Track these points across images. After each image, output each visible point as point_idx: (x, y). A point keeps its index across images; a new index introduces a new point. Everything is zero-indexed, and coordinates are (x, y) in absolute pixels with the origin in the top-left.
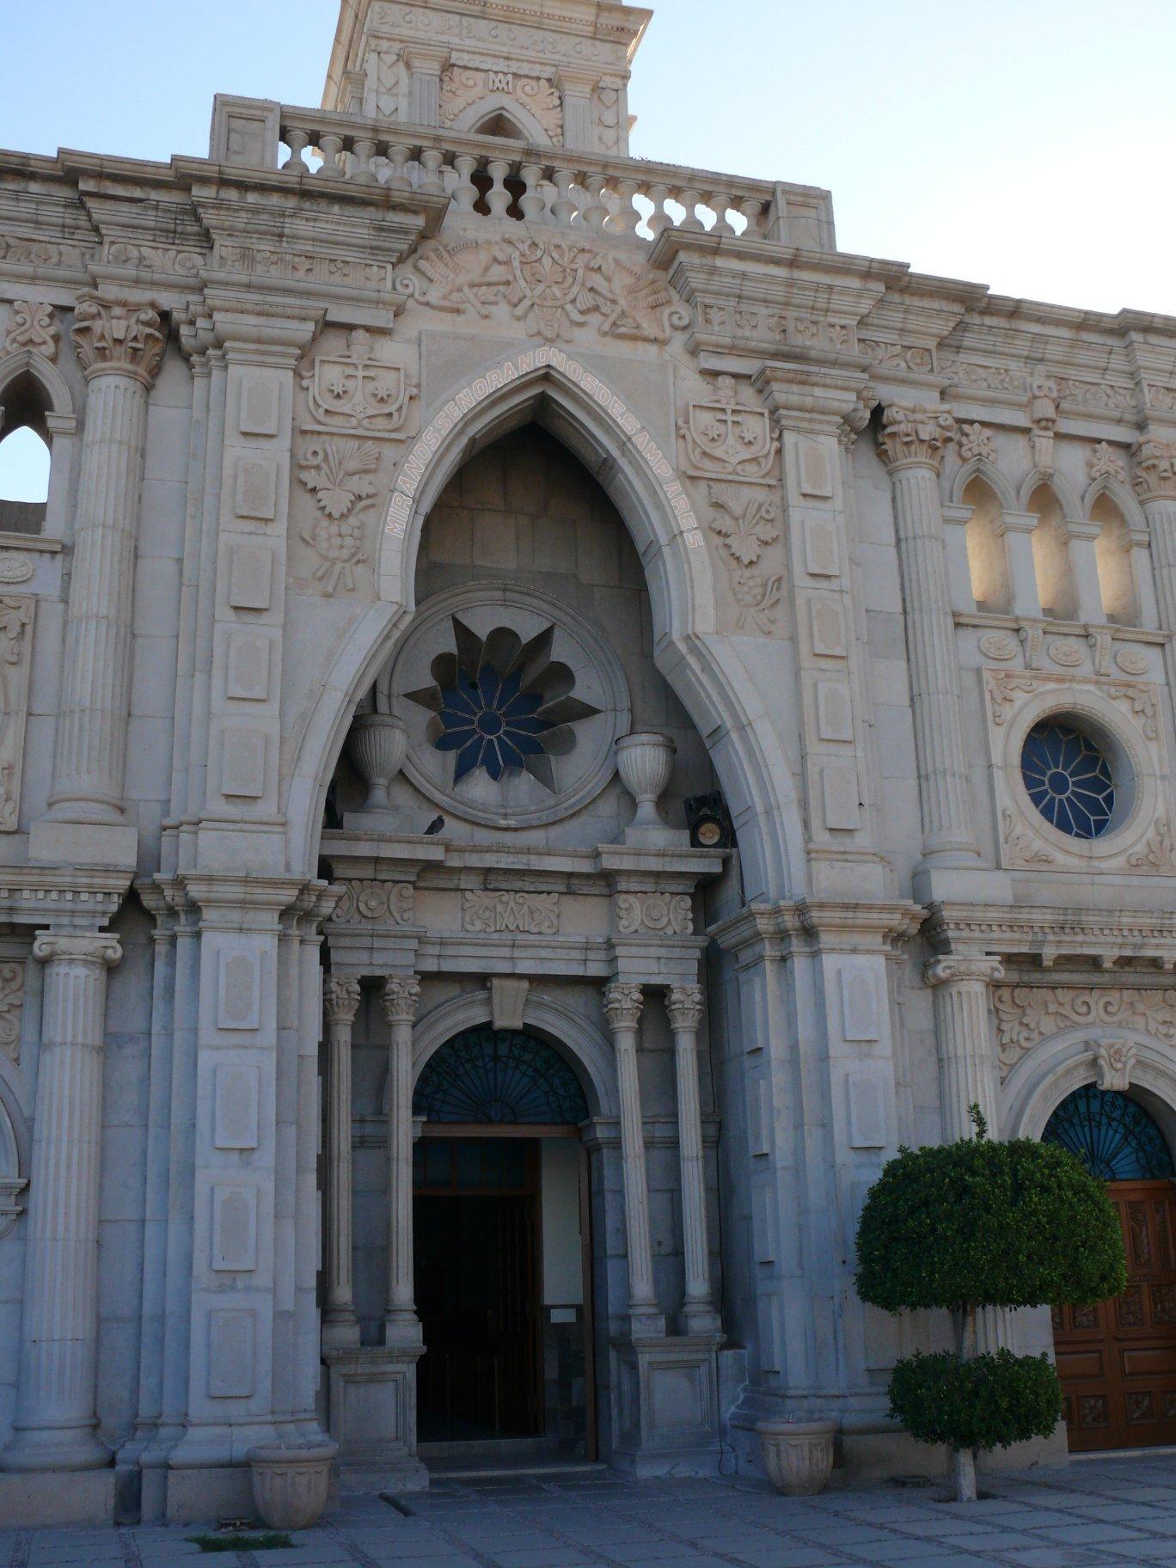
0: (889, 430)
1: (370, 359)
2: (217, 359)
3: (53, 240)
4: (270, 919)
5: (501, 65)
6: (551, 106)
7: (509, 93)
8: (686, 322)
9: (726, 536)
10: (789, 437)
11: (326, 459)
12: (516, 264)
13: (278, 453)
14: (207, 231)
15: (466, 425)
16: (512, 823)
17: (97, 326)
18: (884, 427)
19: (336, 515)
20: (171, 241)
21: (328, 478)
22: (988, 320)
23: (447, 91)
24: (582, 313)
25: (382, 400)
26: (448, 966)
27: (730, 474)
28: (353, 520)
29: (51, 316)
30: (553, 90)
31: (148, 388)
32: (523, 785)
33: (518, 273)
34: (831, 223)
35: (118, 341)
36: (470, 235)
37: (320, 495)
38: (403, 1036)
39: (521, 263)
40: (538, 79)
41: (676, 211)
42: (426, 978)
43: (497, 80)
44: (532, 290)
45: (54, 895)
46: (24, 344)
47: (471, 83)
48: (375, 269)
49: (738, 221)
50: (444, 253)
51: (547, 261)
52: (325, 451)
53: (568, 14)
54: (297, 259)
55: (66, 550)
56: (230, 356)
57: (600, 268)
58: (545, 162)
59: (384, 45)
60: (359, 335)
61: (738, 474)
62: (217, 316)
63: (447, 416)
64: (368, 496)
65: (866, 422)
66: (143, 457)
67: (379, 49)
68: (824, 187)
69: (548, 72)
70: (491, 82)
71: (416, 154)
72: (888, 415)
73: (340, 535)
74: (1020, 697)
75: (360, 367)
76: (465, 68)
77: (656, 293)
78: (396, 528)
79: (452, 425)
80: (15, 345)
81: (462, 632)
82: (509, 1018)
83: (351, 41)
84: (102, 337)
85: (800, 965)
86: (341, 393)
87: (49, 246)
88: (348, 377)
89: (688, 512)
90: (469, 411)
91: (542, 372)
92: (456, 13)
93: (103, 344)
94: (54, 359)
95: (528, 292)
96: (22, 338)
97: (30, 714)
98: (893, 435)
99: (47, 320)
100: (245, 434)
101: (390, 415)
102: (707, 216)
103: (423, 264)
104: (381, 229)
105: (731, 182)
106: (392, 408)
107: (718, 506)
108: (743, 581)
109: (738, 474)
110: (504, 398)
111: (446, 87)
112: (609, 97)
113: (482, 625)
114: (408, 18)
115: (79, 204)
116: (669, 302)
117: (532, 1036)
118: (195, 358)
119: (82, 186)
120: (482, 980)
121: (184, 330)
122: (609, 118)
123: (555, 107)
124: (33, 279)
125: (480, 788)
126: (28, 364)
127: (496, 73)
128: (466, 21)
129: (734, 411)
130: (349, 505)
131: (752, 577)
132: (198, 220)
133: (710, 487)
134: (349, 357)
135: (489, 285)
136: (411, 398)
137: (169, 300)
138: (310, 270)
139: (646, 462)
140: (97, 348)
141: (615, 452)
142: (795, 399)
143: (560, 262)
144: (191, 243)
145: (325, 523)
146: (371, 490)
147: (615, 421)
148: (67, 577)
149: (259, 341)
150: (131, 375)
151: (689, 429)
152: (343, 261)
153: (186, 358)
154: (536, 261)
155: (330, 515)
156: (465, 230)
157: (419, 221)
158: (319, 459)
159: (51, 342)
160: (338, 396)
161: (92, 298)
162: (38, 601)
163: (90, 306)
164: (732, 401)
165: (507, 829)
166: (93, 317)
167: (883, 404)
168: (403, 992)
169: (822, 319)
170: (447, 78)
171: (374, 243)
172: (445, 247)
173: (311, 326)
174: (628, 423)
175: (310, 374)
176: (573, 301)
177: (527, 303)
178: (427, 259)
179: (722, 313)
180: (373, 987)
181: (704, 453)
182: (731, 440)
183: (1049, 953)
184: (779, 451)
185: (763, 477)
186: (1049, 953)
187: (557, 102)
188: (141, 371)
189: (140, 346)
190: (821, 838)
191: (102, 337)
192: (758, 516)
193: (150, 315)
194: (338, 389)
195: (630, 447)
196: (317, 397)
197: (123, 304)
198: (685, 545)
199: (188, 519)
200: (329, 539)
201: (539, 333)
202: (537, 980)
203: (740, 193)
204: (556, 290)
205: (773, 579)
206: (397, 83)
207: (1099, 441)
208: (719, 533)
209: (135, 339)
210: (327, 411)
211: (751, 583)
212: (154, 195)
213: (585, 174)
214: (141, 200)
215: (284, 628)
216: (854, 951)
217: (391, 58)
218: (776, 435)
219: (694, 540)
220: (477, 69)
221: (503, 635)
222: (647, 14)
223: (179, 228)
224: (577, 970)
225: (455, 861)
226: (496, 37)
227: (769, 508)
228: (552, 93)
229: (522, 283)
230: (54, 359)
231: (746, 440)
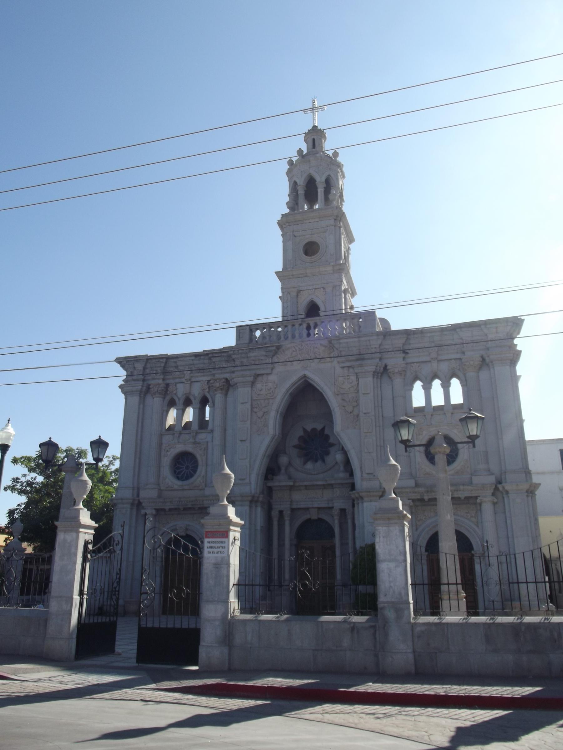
0: (389, 371)
4: (247, 503)
10: (360, 380)
12: (298, 351)
13: (248, 406)
15: (288, 391)
16: (315, 473)
17: (214, 385)
18: (388, 370)
19: (260, 417)
22: (416, 336)
26: (299, 507)
28: (263, 418)
29: (208, 383)
32: (319, 463)
33: (298, 353)
37: (258, 413)
38: (287, 523)
40: (321, 288)
42: (293, 510)
45: (210, 501)
52: (258, 404)
55: (212, 431)
58: (307, 322)
60: (265, 376)
64: (267, 412)
65: (382, 371)
72: (388, 367)
74: (425, 433)
81: (305, 430)
82: (314, 517)
84: (215, 387)
85: (360, 504)
94: (208, 392)
97: (207, 465)
98: (389, 372)
101: (270, 393)
104: (267, 352)
106: (271, 391)
107: (343, 400)
110: (296, 383)
111: (299, 297)
113: (309, 428)
115: (210, 358)
117: (320, 520)
119: (209, 356)
120: (307, 509)
124: (204, 376)
125: (309, 465)
137: (227, 376)
148: (213, 437)
152: (262, 360)
155: (259, 418)
157: (274, 348)
162: (207, 442)
165: (314, 474)
166: (213, 383)
167: (387, 364)
168: (287, 513)
173: (252, 378)
180: (281, 512)
183: (426, 498)
184: (358, 384)
186: (426, 498)
189: (222, 387)
190: (365, 475)
193: (223, 380)
197: (219, 379)
202: (319, 508)
203: (353, 317)
206: (288, 299)
207: (451, 359)
208: (343, 406)
209: (221, 386)
210: (258, 395)
212: (223, 354)
214: (221, 356)
215: (250, 443)
216: (371, 501)
218: (357, 380)
221: (314, 430)
224: (326, 506)
225: (297, 484)
230: (208, 392)
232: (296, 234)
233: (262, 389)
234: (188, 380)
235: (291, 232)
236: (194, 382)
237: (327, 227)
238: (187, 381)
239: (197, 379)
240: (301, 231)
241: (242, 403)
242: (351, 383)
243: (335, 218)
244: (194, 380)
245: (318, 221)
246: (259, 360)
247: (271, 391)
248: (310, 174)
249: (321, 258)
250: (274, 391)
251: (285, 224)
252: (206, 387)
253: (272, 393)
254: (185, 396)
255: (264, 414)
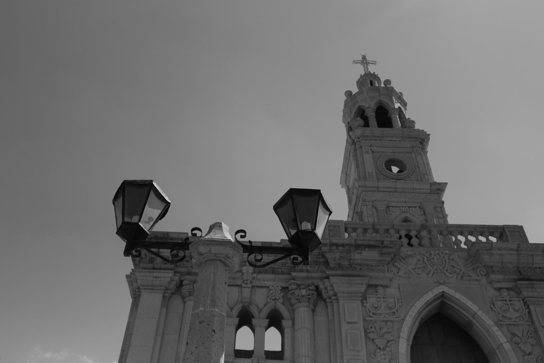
1: (384, 295)
2: (335, 299)
3: (280, 267)
5: (404, 204)
6: (421, 214)
7: (408, 212)
8: (485, 273)
9: (518, 344)
10: (532, 307)
11: (375, 329)
12: (426, 260)
14: (327, 260)
15: (419, 314)
19: (382, 347)
20: (316, 264)
21: (377, 335)
23: (389, 214)
24: (450, 273)
25: (390, 308)
27: (514, 322)
28: (387, 349)
29: (281, 290)
30: (421, 210)
31: (313, 311)
34: (525, 236)
35: (303, 296)
36: (409, 253)
37: (375, 341)
39: (428, 260)
40: (416, 207)
41: (472, 239)
43: (403, 209)
44: (433, 268)
46: (273, 300)
47: (395, 211)
48: (381, 266)
49: (493, 239)
50: (402, 260)
51: (435, 258)
53: (421, 187)
54: (356, 266)
56: (339, 298)
57: (453, 259)
59: (368, 203)
61: (516, 322)
62: (334, 286)
63: (413, 311)
66: (314, 333)
67: (366, 204)
68: (520, 225)
69: (418, 205)
70: (402, 210)
71: (387, 231)
73: (384, 354)
75: (382, 298)
76: (393, 207)
77: (473, 264)
78: (402, 350)
79: (415, 314)
80: (271, 300)
83: (355, 205)
84: (298, 296)
86: (377, 307)
87: (278, 269)
88: (378, 301)
89: (502, 336)
90: (420, 309)
91: (441, 294)
92: (388, 192)
93: (299, 297)
95: (431, 268)
96: (273, 298)
99: (280, 292)
100: (348, 323)
101: (394, 313)
102: (483, 239)
103: (396, 264)
105: (489, 227)
106: (395, 310)
107: (514, 334)
108: (529, 360)
109: (516, 322)
110: (430, 304)
111: (388, 213)
112: (439, 209)
114: (373, 195)
116: (478, 267)
118: (328, 300)
121: (323, 291)
122: (440, 215)
123: (423, 215)
126: (275, 306)
127: (403, 207)
128: (391, 194)
129: (510, 301)
130: (386, 344)
131: (532, 358)
132: (324, 256)
133: (508, 327)
134: (377, 295)
135: (418, 268)
136: (400, 306)
138: (360, 269)
139: (483, 320)
140: (297, 299)
141: (471, 319)
142: (530, 294)
143: (440, 258)
144: (322, 264)
145: (378, 351)
146: (392, 338)
147: (469, 308)
149: (348, 293)
150: (308, 307)
151: (495, 308)
152: (372, 265)
153: (325, 301)
154: (432, 259)
155: (380, 348)
156: (407, 251)
158: (373, 329)
159: (282, 298)
160: (376, 308)
161: (295, 283)
163: (294, 286)
164: (508, 297)
169: (531, 266)
170: (388, 210)
171: (380, 258)
172: (402, 257)
173: (365, 286)
174: (475, 308)
175: (366, 301)
176: (447, 270)
177: (432, 272)
178: (397, 262)
179: (497, 268)
181: (503, 316)
182: (511, 310)
184: (529, 312)
185: (526, 322)
187: (423, 213)
188: (311, 306)
189: (311, 297)
191: (298, 296)
192: (528, 336)
194: (376, 305)
195: (476, 316)
196: (369, 308)
198: (504, 349)
199: (332, 353)
200: (381, 355)
201: (438, 281)
203: (492, 230)
204: (440, 267)
205: (540, 358)
206: (373, 213)
209: (309, 295)
210: (373, 313)
211: (532, 361)
213: (441, 231)
217: (370, 207)
218: (526, 307)
219: (507, 346)
220: (397, 207)
222: (446, 184)
223: (318, 260)
226: (401, 197)
227: (531, 333)
228: (421, 211)
229: (429, 266)
230: (283, 304)
231: (516, 310)
232: (374, 149)
233: (378, 306)
234: (249, 282)
235: (368, 146)
236: (257, 287)
237: (413, 147)
238: (247, 284)
239: (263, 284)
240: (380, 147)
241: (348, 323)
242: (518, 311)
243: (421, 141)
244: (257, 284)
245: (400, 141)
246: (367, 265)
247: (395, 310)
248: (381, 100)
249: (409, 177)
250: (399, 310)
251: (359, 138)
252: (279, 295)
253: (396, 312)
254: (241, 305)
255: (387, 344)
